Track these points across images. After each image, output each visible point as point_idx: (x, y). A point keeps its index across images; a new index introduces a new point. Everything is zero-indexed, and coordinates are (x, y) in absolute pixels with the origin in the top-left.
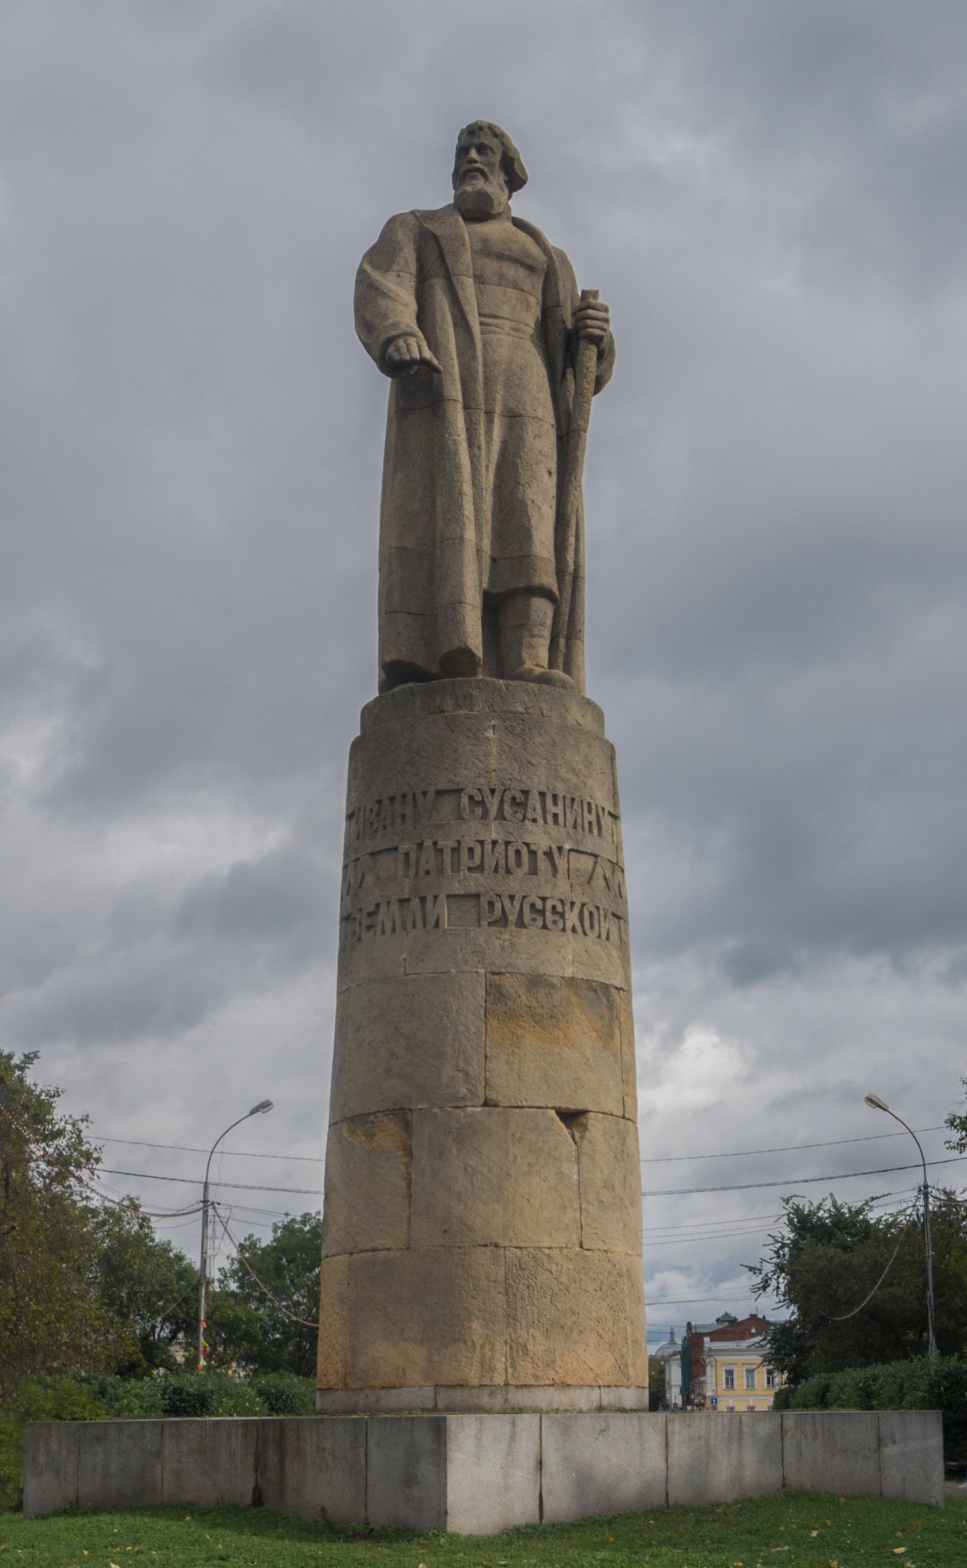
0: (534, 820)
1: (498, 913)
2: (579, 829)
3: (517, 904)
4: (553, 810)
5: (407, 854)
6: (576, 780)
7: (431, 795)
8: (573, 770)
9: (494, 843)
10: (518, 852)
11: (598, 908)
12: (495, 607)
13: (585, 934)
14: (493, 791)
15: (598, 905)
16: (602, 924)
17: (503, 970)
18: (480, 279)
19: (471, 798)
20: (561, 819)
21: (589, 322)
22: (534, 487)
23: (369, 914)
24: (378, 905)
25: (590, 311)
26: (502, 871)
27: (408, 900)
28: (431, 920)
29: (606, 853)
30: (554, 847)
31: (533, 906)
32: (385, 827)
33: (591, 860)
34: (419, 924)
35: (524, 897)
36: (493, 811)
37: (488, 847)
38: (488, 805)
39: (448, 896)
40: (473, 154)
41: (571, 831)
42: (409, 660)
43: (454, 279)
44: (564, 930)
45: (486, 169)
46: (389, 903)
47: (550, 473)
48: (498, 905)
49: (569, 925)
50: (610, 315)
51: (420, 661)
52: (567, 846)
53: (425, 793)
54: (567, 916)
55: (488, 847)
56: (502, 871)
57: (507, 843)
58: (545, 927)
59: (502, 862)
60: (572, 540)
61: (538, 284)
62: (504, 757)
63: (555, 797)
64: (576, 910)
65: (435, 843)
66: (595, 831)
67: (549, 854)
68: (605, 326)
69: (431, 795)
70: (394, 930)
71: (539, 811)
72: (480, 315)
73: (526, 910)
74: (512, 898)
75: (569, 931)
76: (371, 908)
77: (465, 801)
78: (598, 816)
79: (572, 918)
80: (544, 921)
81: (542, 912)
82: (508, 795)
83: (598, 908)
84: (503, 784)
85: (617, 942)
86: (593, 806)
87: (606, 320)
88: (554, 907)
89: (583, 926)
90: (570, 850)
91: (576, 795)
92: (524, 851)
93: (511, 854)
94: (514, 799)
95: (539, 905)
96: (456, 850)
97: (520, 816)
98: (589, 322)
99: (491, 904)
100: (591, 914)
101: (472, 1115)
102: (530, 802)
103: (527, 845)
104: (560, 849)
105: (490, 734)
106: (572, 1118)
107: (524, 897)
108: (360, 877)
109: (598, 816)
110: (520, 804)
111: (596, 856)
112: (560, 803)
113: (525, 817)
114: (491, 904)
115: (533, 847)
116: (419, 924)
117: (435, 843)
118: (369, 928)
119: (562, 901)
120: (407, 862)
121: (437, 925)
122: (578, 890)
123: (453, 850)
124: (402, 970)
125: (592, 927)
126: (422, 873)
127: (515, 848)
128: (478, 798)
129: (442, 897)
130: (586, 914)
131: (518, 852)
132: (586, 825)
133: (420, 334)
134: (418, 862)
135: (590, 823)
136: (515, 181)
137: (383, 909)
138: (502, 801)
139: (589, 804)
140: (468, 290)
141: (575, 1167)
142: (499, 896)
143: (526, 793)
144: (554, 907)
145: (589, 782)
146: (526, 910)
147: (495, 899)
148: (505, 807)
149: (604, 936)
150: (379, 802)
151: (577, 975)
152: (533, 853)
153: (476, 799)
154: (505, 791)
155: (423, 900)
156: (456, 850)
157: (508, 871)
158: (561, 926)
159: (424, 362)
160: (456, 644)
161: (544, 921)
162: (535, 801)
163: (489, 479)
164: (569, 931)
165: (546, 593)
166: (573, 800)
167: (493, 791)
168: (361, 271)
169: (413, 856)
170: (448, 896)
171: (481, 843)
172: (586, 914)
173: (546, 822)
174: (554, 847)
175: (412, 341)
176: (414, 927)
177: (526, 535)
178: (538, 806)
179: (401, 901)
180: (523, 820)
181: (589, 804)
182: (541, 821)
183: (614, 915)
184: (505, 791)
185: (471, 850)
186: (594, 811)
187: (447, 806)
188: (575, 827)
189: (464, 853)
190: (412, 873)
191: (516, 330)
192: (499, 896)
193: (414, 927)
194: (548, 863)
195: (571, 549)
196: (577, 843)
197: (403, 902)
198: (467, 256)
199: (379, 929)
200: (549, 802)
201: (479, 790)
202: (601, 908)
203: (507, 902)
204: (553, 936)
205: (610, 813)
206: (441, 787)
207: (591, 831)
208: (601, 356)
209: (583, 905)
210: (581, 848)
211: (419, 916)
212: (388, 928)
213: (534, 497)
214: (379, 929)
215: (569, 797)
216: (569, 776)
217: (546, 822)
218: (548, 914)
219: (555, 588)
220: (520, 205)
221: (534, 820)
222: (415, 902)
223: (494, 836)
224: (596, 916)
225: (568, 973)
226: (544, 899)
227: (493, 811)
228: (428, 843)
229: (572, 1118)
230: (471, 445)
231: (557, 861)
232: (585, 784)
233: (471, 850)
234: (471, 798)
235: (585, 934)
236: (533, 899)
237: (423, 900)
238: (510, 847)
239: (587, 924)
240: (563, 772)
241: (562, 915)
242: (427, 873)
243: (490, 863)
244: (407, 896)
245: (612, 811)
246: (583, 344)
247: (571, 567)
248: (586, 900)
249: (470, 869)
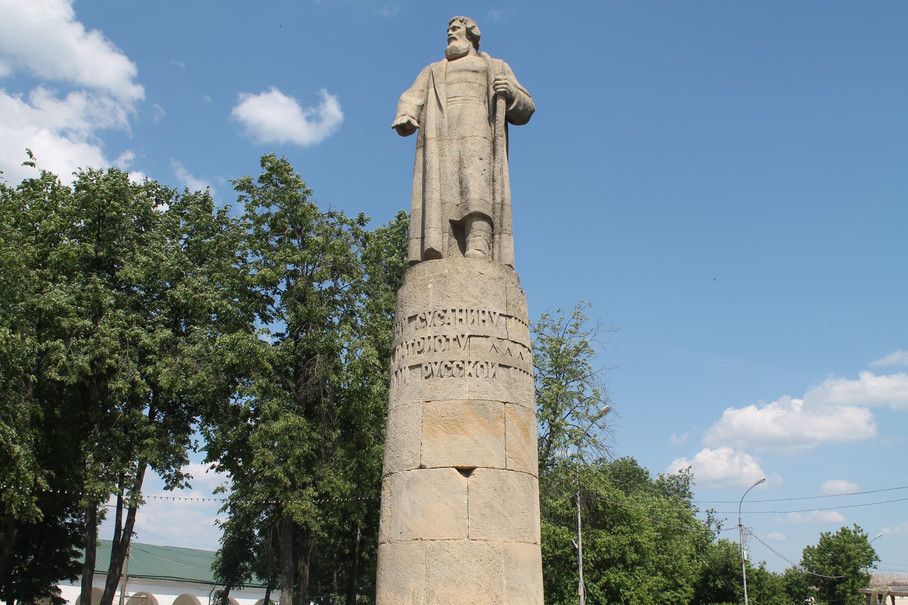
1: (429, 371)
6: (475, 301)
7: (407, 320)
8: (473, 296)
9: (429, 338)
30: (460, 336)
37: (427, 340)
41: (470, 326)
48: (429, 368)
52: (467, 335)
61: (481, 79)
64: (472, 365)
74: (436, 363)
79: (468, 369)
82: (437, 313)
90: (469, 336)
95: (449, 365)
99: (426, 368)
100: (482, 366)
101: (413, 474)
106: (466, 471)
114: (426, 368)
119: (463, 362)
122: (473, 355)
139: (483, 312)
141: (466, 497)
143: (445, 311)
152: (448, 340)
166: (472, 311)
174: (460, 336)
183: (500, 365)
186: (487, 312)
204: (457, 381)
205: (501, 315)
206: (410, 315)
216: (471, 299)
225: (466, 397)
226: (452, 362)
227: (429, 322)
229: (466, 471)
240: (466, 298)
243: (426, 349)
245: (505, 313)
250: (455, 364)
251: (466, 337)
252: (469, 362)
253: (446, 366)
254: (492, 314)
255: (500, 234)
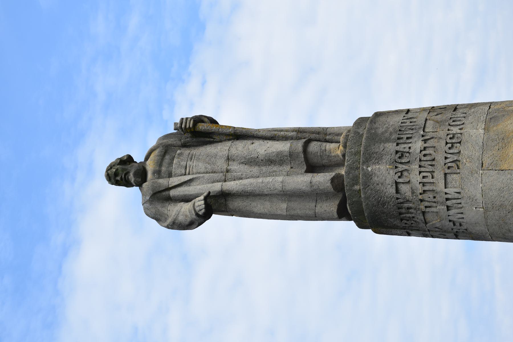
0: (410, 148)
2: (414, 127)
3: (449, 156)
4: (405, 139)
5: (426, 207)
7: (398, 196)
10: (425, 155)
11: (451, 118)
12: (312, 168)
13: (463, 124)
14: (396, 167)
15: (449, 118)
16: (459, 116)
17: (481, 162)
18: (170, 175)
19: (399, 177)
20: (408, 136)
21: (187, 127)
22: (259, 150)
23: (454, 225)
24: (450, 221)
25: (183, 126)
26: (433, 163)
27: (448, 207)
28: (457, 195)
29: (425, 115)
30: (422, 138)
31: (450, 148)
32: (413, 217)
33: (428, 122)
34: (459, 201)
35: (446, 152)
36: (405, 167)
37: (422, 169)
38: (402, 169)
39: (445, 188)
40: (118, 178)
42: (337, 207)
43: (170, 186)
44: (461, 134)
45: (125, 172)
46: (449, 216)
47: (252, 143)
48: (450, 165)
49: (459, 131)
50: (184, 117)
51: (337, 202)
52: (422, 133)
53: (397, 199)
54: (455, 132)
55: (422, 169)
56: (433, 163)
57: (420, 160)
58: (460, 143)
59: (429, 163)
60: (282, 133)
62: (380, 162)
63: (399, 139)
64: (452, 128)
65: (421, 194)
66: (415, 120)
67: (425, 141)
68: (189, 119)
69: (398, 196)
70: (462, 213)
71: (405, 145)
72: (185, 175)
73: (451, 151)
74: (446, 158)
75: (462, 131)
76: (451, 224)
77: (400, 180)
78: (408, 119)
79: (455, 130)
80: (457, 143)
81: (452, 143)
83: (451, 118)
84: (393, 163)
85: (468, 109)
86: (403, 121)
87: (187, 118)
88: (450, 138)
89: (459, 125)
90: (424, 131)
91: (397, 129)
92: (424, 152)
93: (425, 158)
94: (400, 158)
95: (449, 145)
96: (424, 184)
97: (407, 155)
98: (187, 127)
99: (449, 168)
100: (453, 121)
102: (401, 150)
103: (421, 151)
104: (423, 136)
105: (370, 169)
107: (446, 152)
108: (437, 229)
109: (408, 119)
110: (402, 155)
111: (426, 120)
112: (402, 136)
113: (408, 152)
114: (449, 168)
115: (422, 149)
116: (459, 201)
117: (421, 194)
118: (461, 225)
119: (448, 135)
120: (430, 207)
121: (459, 193)
123: (423, 186)
124: (481, 209)
125: (460, 121)
126: (435, 200)
127: (423, 157)
128: (399, 174)
129: (446, 190)
130: (454, 123)
131: (425, 155)
132: (412, 124)
133: (193, 201)
134: (430, 202)
135: (411, 122)
136: (128, 160)
137: (451, 218)
138: (401, 163)
140: (174, 181)
142: (445, 164)
143: (397, 152)
144: (450, 138)
145: (391, 123)
146: (451, 151)
147: (447, 166)
148: (403, 161)
149: (465, 115)
150: (402, 220)
151: (483, 127)
152: (425, 149)
153: (400, 175)
154: (396, 162)
155: (447, 199)
156: (424, 184)
157: (434, 160)
158: (459, 135)
159: (205, 199)
160: (329, 184)
161: (457, 143)
162: (401, 148)
163: (255, 170)
164: (462, 131)
165: (306, 145)
166: (400, 130)
167: (396, 167)
168: (168, 227)
169: (427, 204)
170: (445, 188)
171: (420, 172)
172: (454, 123)
173: (411, 143)
174: (422, 138)
175: (196, 204)
176: (460, 203)
177: (279, 154)
178: (403, 146)
179: (448, 210)
180: (409, 153)
181: (402, 123)
182: (410, 145)
184: (396, 162)
185: (424, 177)
187: (404, 188)
188: (413, 129)
189: (425, 180)
190: (434, 205)
191: (191, 159)
192: (445, 164)
193: (460, 203)
194: (429, 141)
195: (286, 133)
196: (420, 128)
197: (448, 208)
198: (161, 181)
199: (461, 220)
200: (401, 141)
201: (396, 173)
202: (451, 116)
203: (448, 161)
204: (464, 138)
207: (415, 122)
208: (203, 122)
209: (449, 125)
210: (423, 126)
211: (454, 201)
212: (460, 216)
213: (263, 151)
214: (461, 220)
215: (398, 132)
217: (411, 143)
218: (454, 141)
219: (304, 140)
220: (139, 158)
221: (410, 148)
222: (449, 203)
223: (417, 167)
224: (455, 119)
225: (482, 131)
226: (447, 143)
228: (420, 197)
230: (241, 179)
231: (428, 137)
232: (392, 125)
233: (424, 177)
234: (399, 177)
235: (463, 124)
236: (446, 148)
237: (447, 199)
238: (422, 159)
239: (458, 123)
241: (454, 135)
242: (434, 197)
243: (430, 169)
244: (446, 207)
246: (197, 130)
247: (294, 134)
248: (447, 123)
249: (433, 178)
250: (449, 141)
251: (424, 134)
252: (449, 130)
253: (450, 148)
254: (405, 118)
255: (326, 134)
